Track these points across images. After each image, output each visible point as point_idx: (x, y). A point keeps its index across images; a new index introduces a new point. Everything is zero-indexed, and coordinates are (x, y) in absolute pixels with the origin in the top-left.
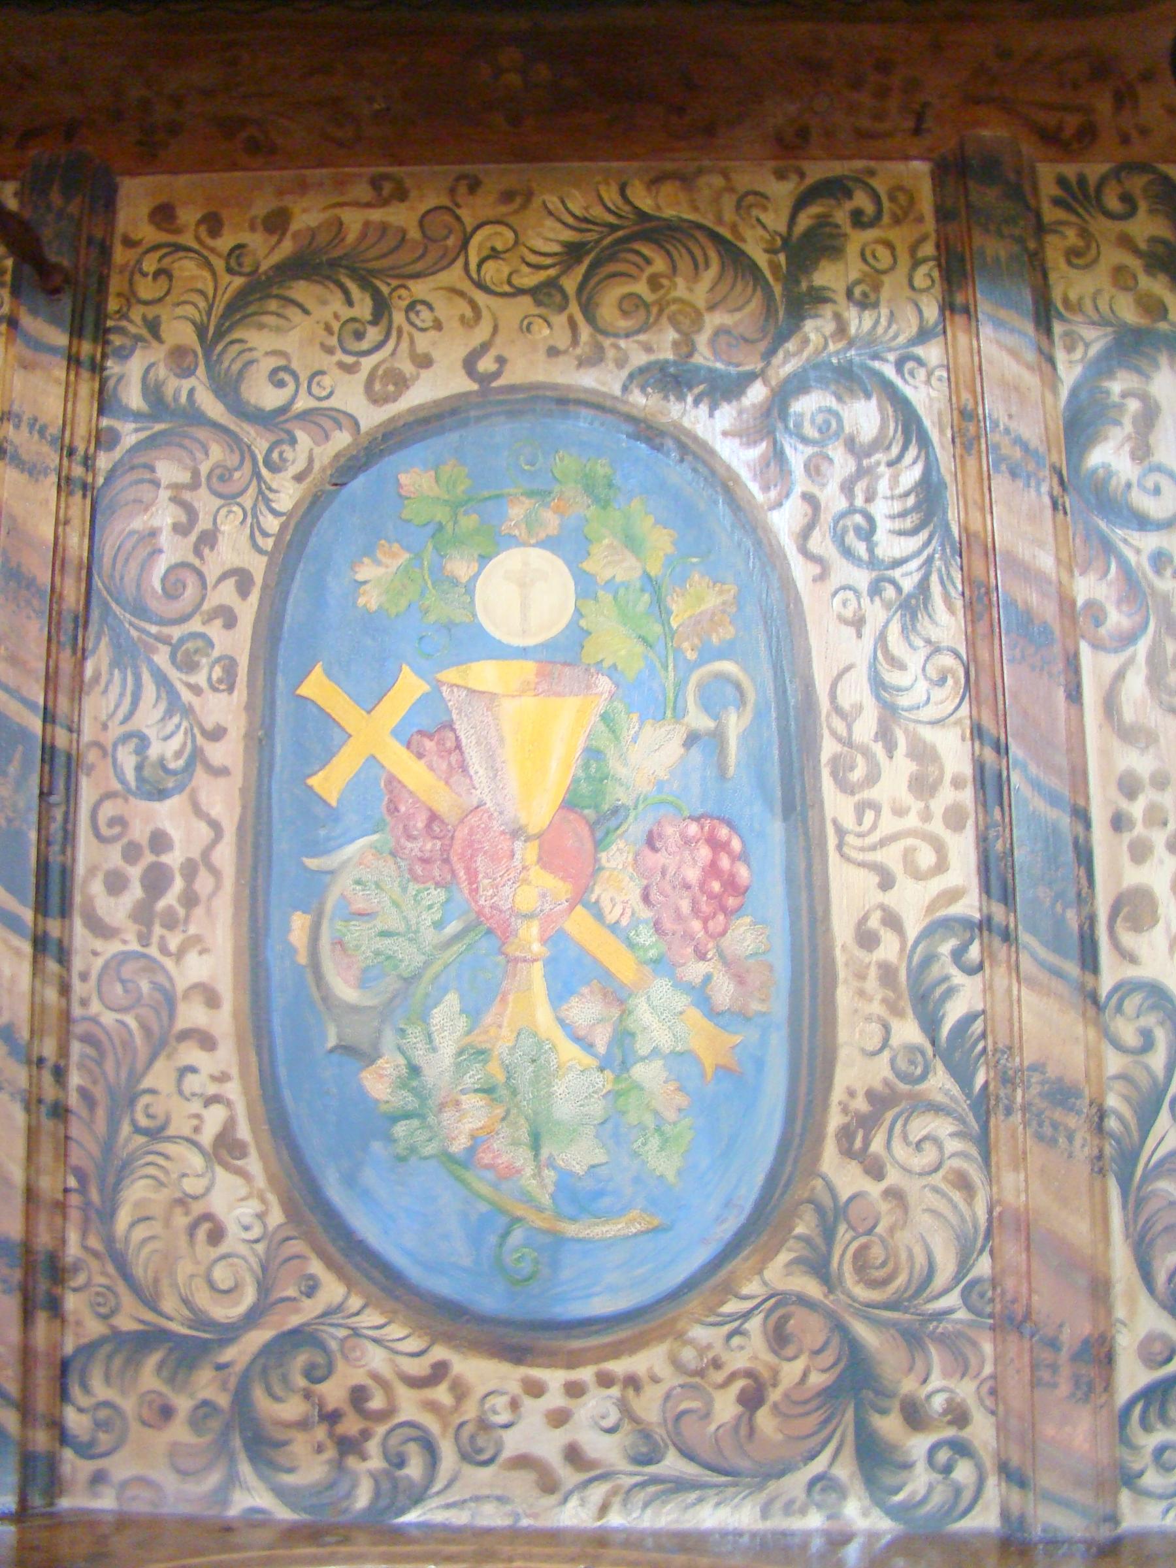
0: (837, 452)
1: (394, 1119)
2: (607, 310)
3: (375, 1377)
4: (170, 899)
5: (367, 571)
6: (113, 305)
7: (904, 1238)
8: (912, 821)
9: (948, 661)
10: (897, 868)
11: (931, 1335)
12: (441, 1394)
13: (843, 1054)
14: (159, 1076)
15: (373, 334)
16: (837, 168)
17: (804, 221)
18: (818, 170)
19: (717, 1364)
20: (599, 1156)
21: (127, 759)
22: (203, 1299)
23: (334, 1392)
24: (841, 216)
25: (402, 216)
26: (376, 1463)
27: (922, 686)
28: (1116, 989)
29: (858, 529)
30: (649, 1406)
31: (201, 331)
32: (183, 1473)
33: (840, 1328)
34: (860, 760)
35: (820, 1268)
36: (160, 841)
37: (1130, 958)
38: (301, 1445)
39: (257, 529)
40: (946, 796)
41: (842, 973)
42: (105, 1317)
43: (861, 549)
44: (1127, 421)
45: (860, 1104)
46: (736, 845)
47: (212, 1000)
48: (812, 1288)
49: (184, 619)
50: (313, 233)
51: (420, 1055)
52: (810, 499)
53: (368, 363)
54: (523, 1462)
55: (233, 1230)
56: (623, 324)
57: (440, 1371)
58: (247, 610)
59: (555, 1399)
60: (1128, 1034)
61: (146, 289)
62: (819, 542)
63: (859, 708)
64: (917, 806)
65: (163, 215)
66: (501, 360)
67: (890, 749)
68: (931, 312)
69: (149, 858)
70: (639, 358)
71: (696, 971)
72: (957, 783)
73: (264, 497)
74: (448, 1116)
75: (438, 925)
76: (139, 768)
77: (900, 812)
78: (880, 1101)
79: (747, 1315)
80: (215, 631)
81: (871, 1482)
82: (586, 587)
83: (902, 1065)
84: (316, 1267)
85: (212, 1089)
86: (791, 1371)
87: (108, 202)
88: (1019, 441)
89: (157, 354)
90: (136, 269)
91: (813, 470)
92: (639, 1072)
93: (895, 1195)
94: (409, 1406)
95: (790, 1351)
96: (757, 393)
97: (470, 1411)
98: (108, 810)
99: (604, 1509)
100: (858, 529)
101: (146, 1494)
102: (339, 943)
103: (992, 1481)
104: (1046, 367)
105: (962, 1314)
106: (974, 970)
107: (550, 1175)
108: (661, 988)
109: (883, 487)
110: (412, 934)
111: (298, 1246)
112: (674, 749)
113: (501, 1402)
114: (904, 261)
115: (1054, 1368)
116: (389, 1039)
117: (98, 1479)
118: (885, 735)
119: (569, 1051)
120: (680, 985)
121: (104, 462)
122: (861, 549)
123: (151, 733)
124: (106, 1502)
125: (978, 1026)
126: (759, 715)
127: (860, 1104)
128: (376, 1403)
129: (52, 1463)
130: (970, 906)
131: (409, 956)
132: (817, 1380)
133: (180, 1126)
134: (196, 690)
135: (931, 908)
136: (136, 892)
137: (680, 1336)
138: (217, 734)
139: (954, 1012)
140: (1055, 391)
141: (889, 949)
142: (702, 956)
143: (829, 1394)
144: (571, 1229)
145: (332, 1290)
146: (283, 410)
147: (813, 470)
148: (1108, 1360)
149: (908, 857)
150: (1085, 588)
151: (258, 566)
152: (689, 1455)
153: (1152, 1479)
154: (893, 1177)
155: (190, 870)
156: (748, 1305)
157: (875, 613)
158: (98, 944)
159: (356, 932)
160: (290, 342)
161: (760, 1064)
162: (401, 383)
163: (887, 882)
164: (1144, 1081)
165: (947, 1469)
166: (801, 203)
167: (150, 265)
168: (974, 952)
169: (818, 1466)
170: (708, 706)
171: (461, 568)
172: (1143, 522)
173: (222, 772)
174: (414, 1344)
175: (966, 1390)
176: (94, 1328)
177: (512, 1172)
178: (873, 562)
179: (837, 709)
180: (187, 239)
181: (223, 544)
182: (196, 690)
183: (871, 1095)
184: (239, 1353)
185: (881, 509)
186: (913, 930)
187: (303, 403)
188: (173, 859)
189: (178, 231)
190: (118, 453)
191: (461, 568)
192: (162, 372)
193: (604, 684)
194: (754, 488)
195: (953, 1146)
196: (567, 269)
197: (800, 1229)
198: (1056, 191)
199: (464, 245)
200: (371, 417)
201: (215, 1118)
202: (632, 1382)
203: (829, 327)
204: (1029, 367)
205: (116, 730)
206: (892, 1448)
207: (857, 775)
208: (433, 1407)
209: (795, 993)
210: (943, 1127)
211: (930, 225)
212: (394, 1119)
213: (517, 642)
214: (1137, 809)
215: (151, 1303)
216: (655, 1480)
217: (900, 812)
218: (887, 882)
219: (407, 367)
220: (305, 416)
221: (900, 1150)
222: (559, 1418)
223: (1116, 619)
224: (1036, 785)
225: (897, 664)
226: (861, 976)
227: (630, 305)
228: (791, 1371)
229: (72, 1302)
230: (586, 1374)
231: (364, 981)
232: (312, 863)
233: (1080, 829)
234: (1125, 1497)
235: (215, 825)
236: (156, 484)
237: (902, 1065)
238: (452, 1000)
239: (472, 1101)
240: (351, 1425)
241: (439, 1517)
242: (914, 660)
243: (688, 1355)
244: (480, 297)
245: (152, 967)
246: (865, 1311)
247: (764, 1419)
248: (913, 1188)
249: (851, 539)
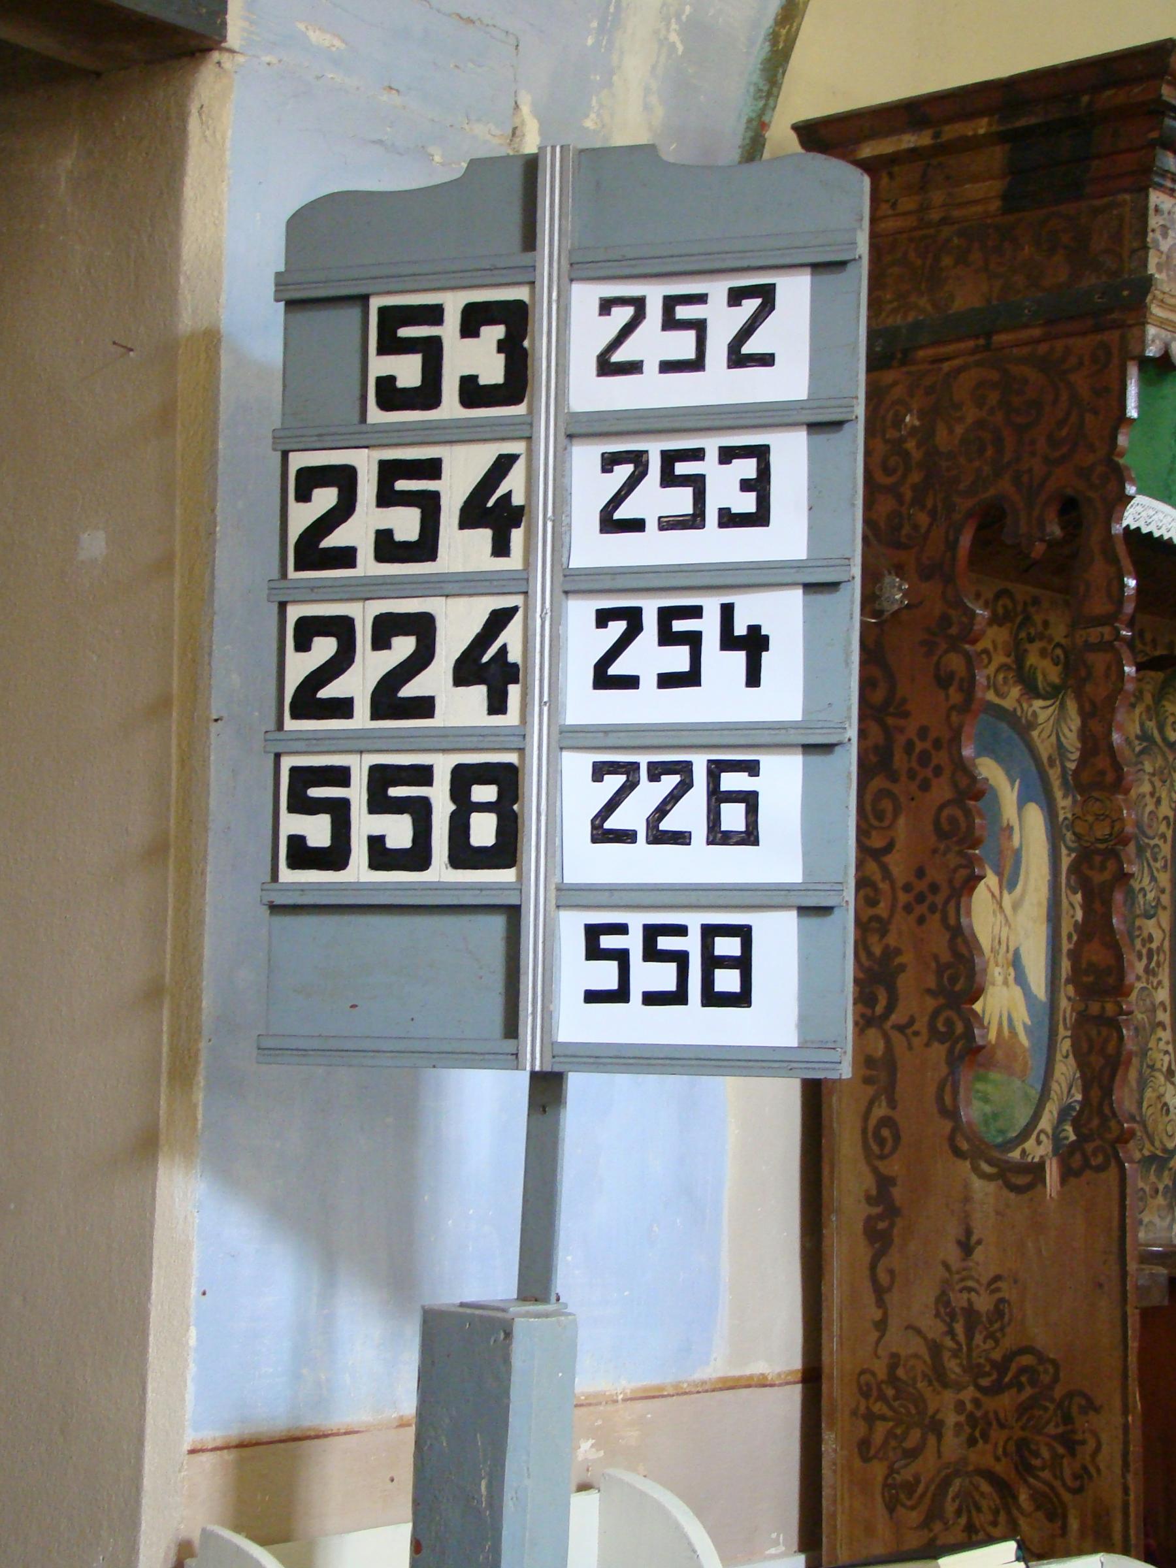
42: (1141, 1150)
76: (1144, 904)
80: (1160, 843)
133: (1158, 1065)
134: (1158, 870)
138: (1163, 891)
173: (1164, 908)
235: (1163, 931)
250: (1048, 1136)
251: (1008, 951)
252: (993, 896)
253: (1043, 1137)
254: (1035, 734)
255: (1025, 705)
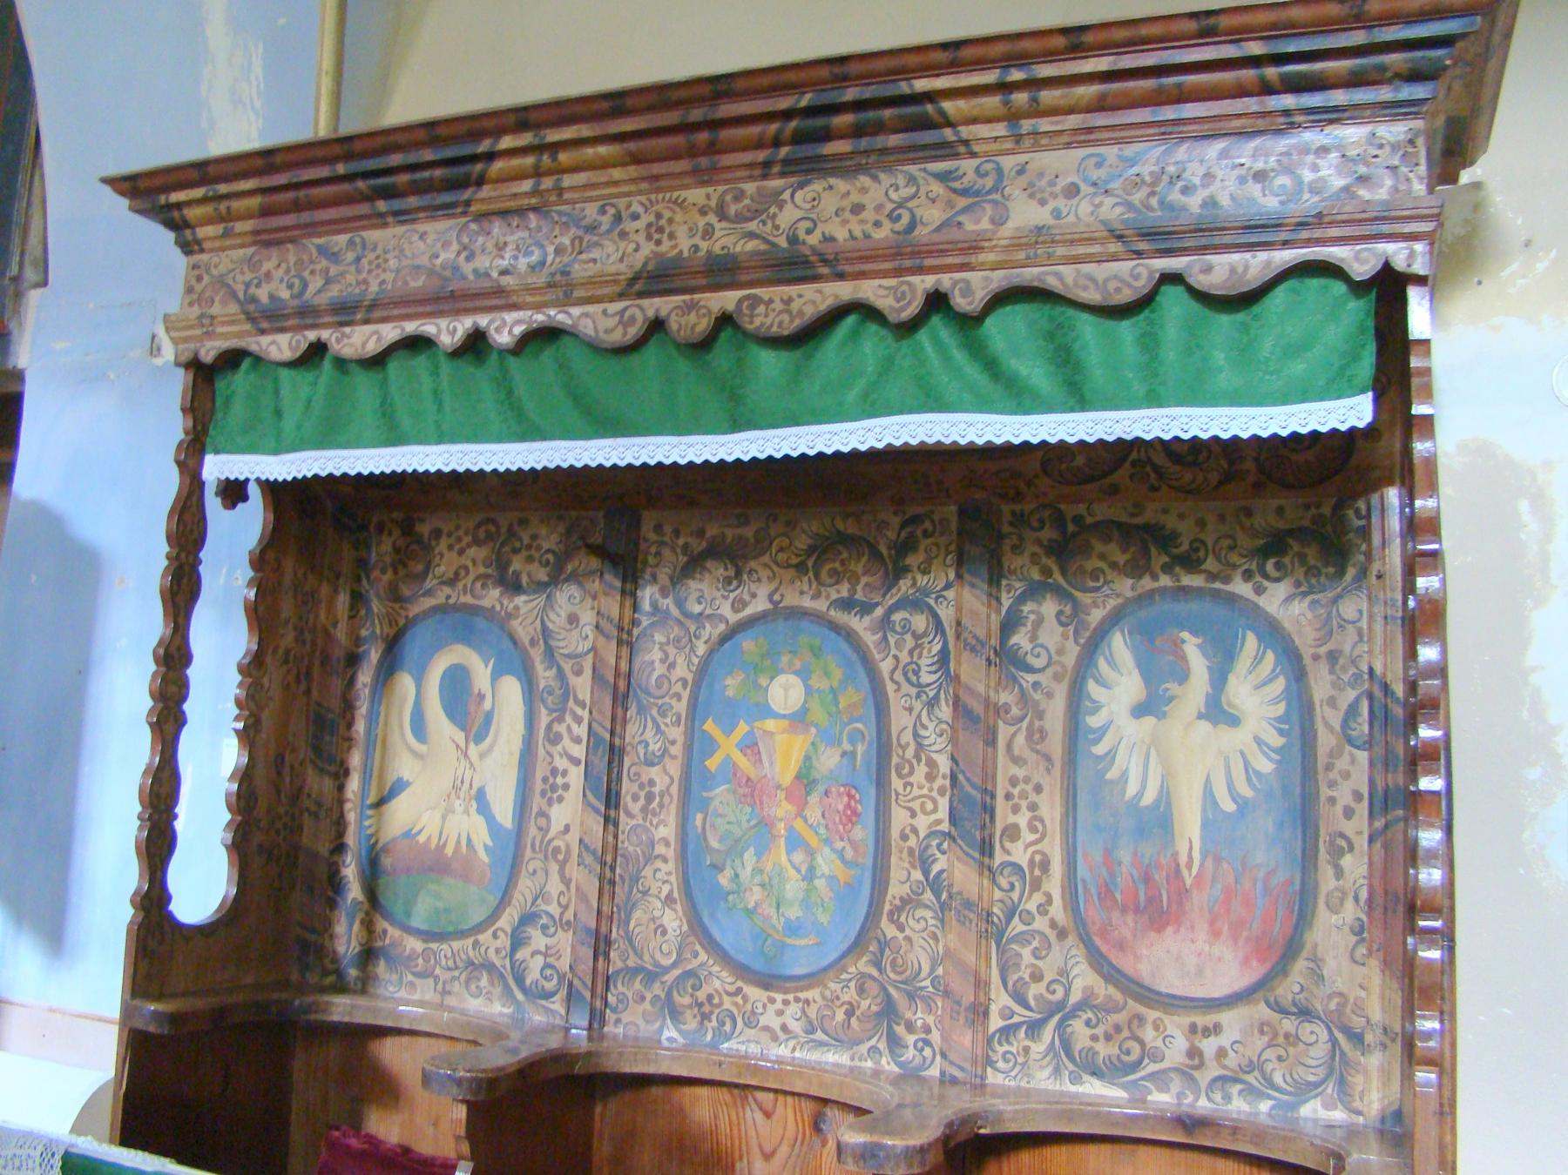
0: (908, 637)
1: (728, 894)
2: (824, 575)
3: (716, 991)
4: (655, 804)
5: (729, 681)
6: (639, 566)
7: (911, 956)
8: (925, 791)
9: (944, 726)
10: (918, 809)
11: (919, 997)
12: (739, 1000)
13: (892, 882)
14: (648, 872)
15: (735, 583)
16: (920, 510)
17: (903, 534)
18: (912, 510)
19: (838, 998)
20: (800, 914)
21: (641, 751)
22: (658, 956)
23: (701, 995)
24: (919, 533)
25: (749, 532)
26: (714, 1023)
27: (934, 736)
28: (1001, 864)
29: (914, 671)
30: (812, 1012)
31: (671, 578)
32: (647, 1022)
33: (885, 989)
34: (907, 766)
35: (877, 964)
36: (652, 783)
37: (1008, 853)
38: (688, 1014)
39: (690, 661)
40: (939, 782)
41: (893, 850)
42: (624, 961)
43: (914, 679)
44: (1029, 624)
45: (897, 902)
46: (857, 796)
47: (667, 844)
48: (875, 973)
49: (663, 697)
50: (714, 537)
51: (739, 870)
52: (896, 657)
53: (732, 595)
54: (766, 1028)
55: (670, 931)
56: (829, 581)
57: (739, 991)
58: (686, 694)
59: (779, 1005)
60: (1004, 883)
61: (651, 560)
62: (898, 676)
63: (908, 744)
64: (927, 785)
65: (658, 528)
66: (782, 596)
67: (919, 761)
68: (952, 575)
69: (647, 789)
70: (834, 596)
71: (839, 845)
72: (944, 777)
73: (692, 650)
74: (747, 894)
75: (748, 821)
77: (921, 787)
78: (905, 901)
79: (850, 980)
80: (674, 702)
81: (891, 1052)
82: (809, 690)
83: (914, 888)
84: (698, 947)
85: (666, 878)
86: (865, 1004)
87: (636, 523)
88: (975, 637)
89: (656, 588)
90: (647, 553)
91: (898, 645)
92: (817, 882)
93: (908, 939)
94: (728, 1003)
95: (865, 996)
96: (879, 611)
97: (749, 1007)
98: (633, 770)
99: (794, 1049)
100: (914, 671)
101: (634, 1028)
102: (713, 826)
103: (938, 1057)
104: (994, 602)
105: (931, 989)
106: (944, 853)
107: (782, 920)
108: (827, 850)
109: (925, 652)
110: (739, 823)
111: (692, 939)
112: (837, 759)
113: (760, 1005)
114: (943, 550)
115: (959, 1014)
116: (729, 862)
117: (618, 1021)
118: (917, 757)
119: (792, 872)
120: (833, 850)
121: (636, 632)
122: (914, 679)
123: (650, 741)
124: (620, 1030)
125: (945, 875)
126: (870, 745)
127: (897, 902)
128: (716, 1001)
129: (603, 1014)
130: (945, 827)
131: (737, 832)
132: (874, 1008)
133: (653, 891)
134: (666, 725)
135: (930, 826)
136: (642, 801)
137: (825, 986)
138: (673, 743)
139: (936, 868)
140: (998, 611)
141: (912, 842)
142: (842, 840)
143: (878, 1014)
144: (788, 941)
145: (703, 956)
146: (700, 614)
147: (898, 645)
148: (986, 1014)
149: (923, 805)
150: (1005, 697)
151: (690, 677)
152: (826, 1033)
153: (1001, 1065)
154: (908, 932)
155: (662, 795)
156: (850, 976)
157: (918, 705)
158: (629, 821)
159: (719, 821)
160: (704, 586)
161: (861, 883)
162: (745, 605)
163: (913, 814)
164: (1009, 903)
165: (922, 1050)
166: (904, 525)
167: (653, 550)
168: (945, 845)
169: (873, 1042)
170: (852, 741)
171: (763, 681)
172: (1030, 669)
173: (674, 757)
174: (730, 980)
175: (930, 1020)
176: (620, 964)
177: (769, 917)
178: (919, 685)
179: (899, 745)
180: (666, 539)
181: (678, 668)
182: (666, 725)
183: (901, 899)
184: (669, 978)
185: (924, 662)
186: (922, 834)
187: (708, 611)
188: (656, 790)
189: (663, 535)
190: (641, 628)
191: (763, 681)
192: (657, 596)
193: (813, 730)
194: (875, 652)
195: (932, 922)
196: (809, 556)
197: (871, 949)
198: (1010, 518)
199: (771, 544)
200: (733, 618)
201: (666, 889)
202: (807, 1002)
203: (909, 582)
204: (983, 604)
205: (637, 739)
206: (900, 1039)
207: (906, 771)
208: (736, 1004)
209: (875, 858)
210: (928, 914)
211: (954, 536)
212: (728, 894)
213: (782, 712)
214: (1016, 791)
215: (641, 958)
216: (812, 1041)
217: (921, 787)
218: (913, 814)
219: (746, 597)
220: (709, 617)
221: (911, 921)
222: (780, 1013)
223: (1015, 711)
224: (968, 780)
225: (925, 728)
226: (901, 852)
227: (834, 573)
228: (865, 1004)
229: (612, 954)
230: (790, 997)
231: (720, 841)
232: (705, 794)
233: (988, 799)
234: (989, 1069)
236: (654, 642)
237: (914, 888)
238: (752, 849)
239: (756, 889)
240: (707, 1009)
241: (735, 1046)
242: (931, 726)
243: (828, 993)
244: (775, 568)
245: (647, 830)
246: (894, 983)
247: (853, 1021)
248: (914, 936)
249: (910, 674)
250: (506, 934)
251: (471, 785)
252: (458, 746)
253: (499, 933)
254: (515, 623)
255: (505, 602)
